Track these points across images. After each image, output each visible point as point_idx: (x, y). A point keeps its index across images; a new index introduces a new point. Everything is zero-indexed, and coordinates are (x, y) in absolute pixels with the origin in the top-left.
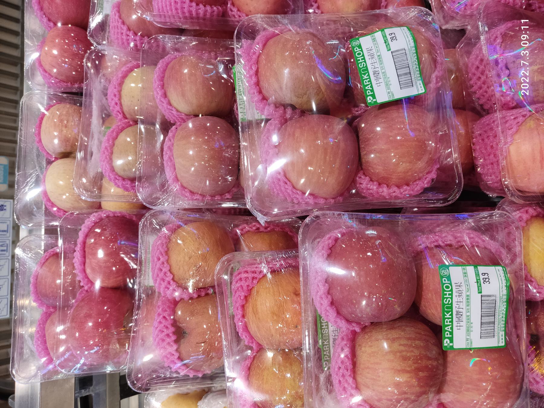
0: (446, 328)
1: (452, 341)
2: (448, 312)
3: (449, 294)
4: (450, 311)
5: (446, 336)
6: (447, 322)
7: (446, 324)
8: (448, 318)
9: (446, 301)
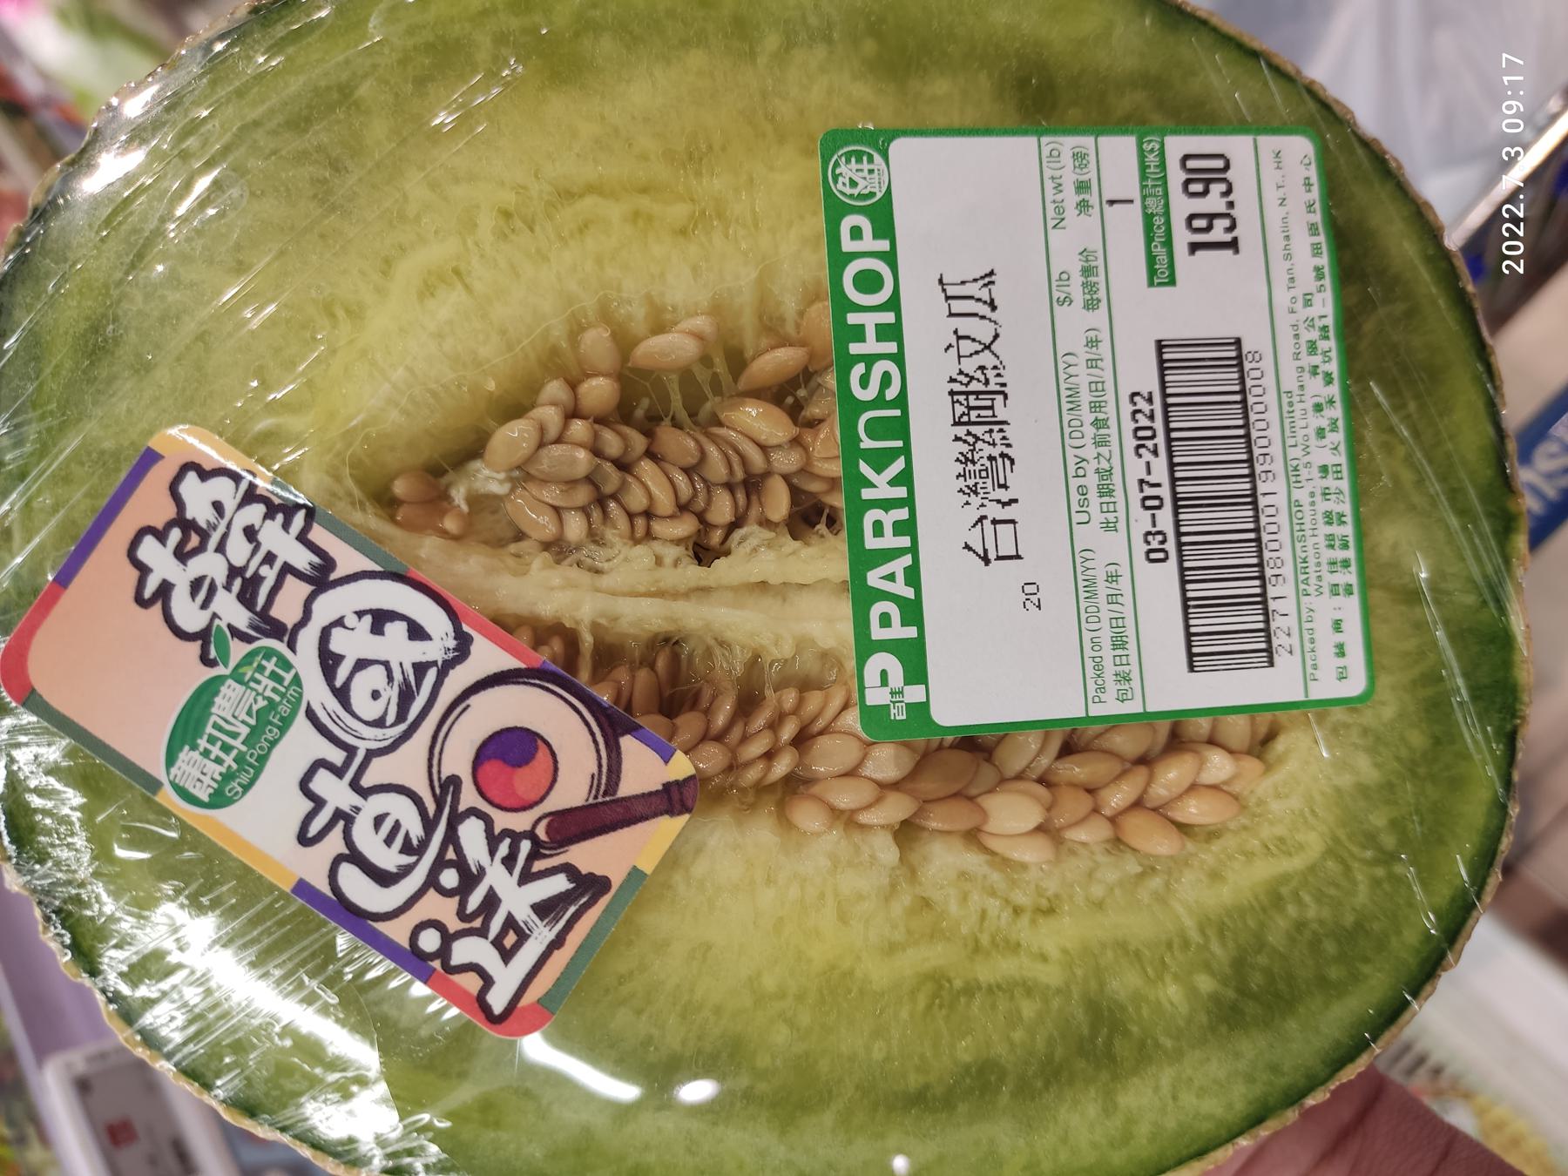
0: (874, 578)
1: (917, 672)
2: (880, 460)
3: (885, 332)
4: (892, 455)
5: (877, 633)
6: (878, 529)
7: (871, 542)
8: (887, 505)
9: (864, 382)
